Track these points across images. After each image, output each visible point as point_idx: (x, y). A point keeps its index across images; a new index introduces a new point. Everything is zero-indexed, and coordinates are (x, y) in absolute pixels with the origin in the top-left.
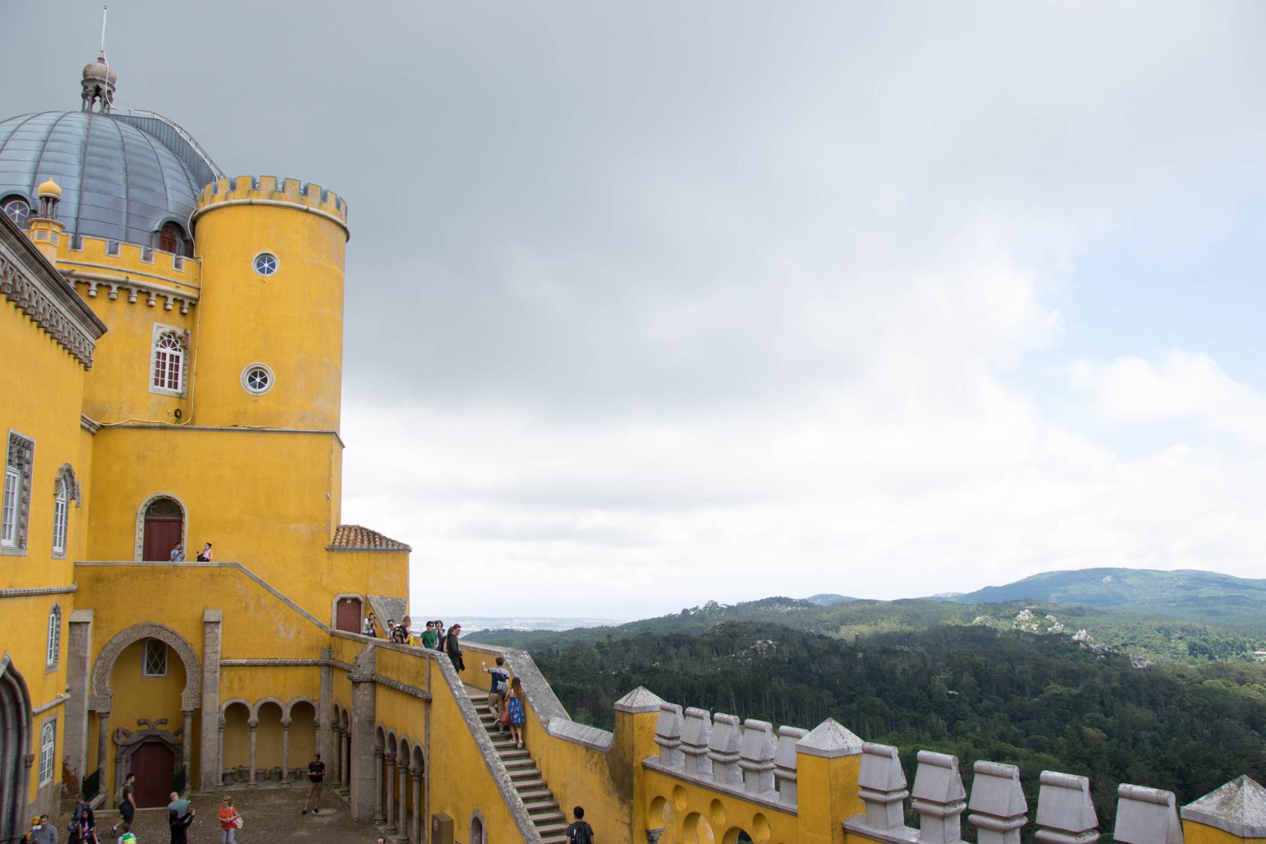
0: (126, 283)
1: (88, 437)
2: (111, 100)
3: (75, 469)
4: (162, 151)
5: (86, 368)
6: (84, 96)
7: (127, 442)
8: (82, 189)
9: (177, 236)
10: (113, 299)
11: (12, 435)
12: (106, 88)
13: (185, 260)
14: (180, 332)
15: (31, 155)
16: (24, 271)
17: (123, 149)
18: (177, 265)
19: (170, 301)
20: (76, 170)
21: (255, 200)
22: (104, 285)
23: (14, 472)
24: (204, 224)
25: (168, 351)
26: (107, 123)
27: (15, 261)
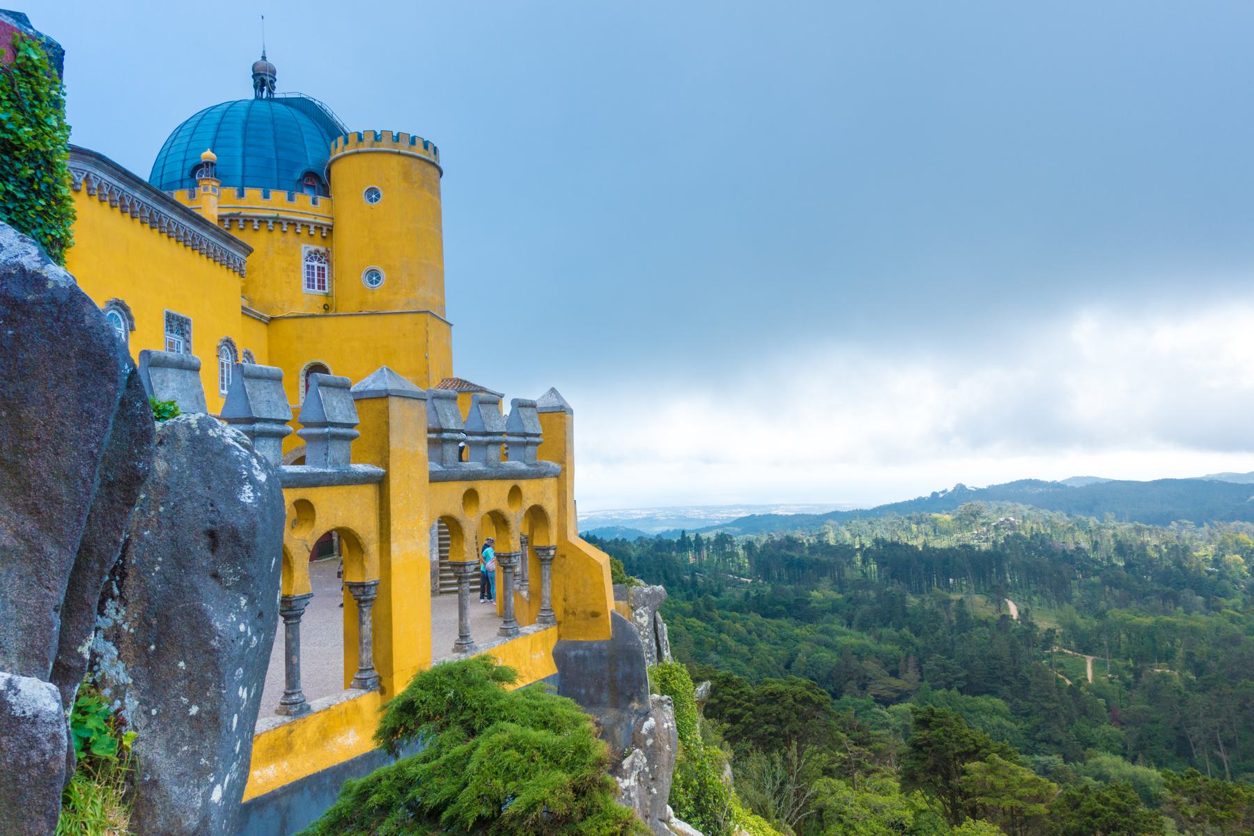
0: (277, 218)
1: (263, 327)
2: (274, 88)
3: (234, 340)
4: (302, 119)
5: (242, 276)
6: (255, 87)
7: (287, 328)
8: (244, 156)
9: (318, 181)
10: (270, 231)
11: (168, 315)
12: (268, 79)
13: (320, 199)
14: (322, 250)
15: (211, 135)
16: (161, 209)
17: (273, 122)
18: (314, 202)
19: (312, 228)
20: (239, 142)
21: (361, 149)
22: (263, 221)
23: (176, 338)
24: (335, 170)
25: (316, 264)
26: (263, 107)
27: (150, 202)
